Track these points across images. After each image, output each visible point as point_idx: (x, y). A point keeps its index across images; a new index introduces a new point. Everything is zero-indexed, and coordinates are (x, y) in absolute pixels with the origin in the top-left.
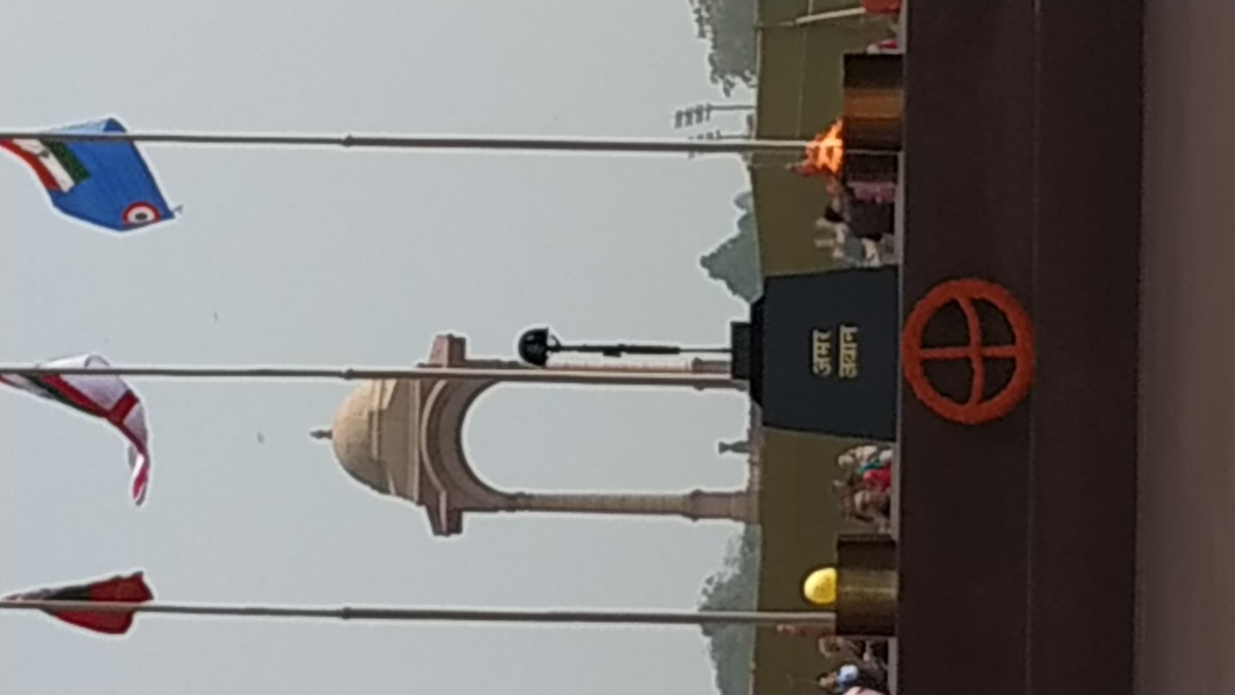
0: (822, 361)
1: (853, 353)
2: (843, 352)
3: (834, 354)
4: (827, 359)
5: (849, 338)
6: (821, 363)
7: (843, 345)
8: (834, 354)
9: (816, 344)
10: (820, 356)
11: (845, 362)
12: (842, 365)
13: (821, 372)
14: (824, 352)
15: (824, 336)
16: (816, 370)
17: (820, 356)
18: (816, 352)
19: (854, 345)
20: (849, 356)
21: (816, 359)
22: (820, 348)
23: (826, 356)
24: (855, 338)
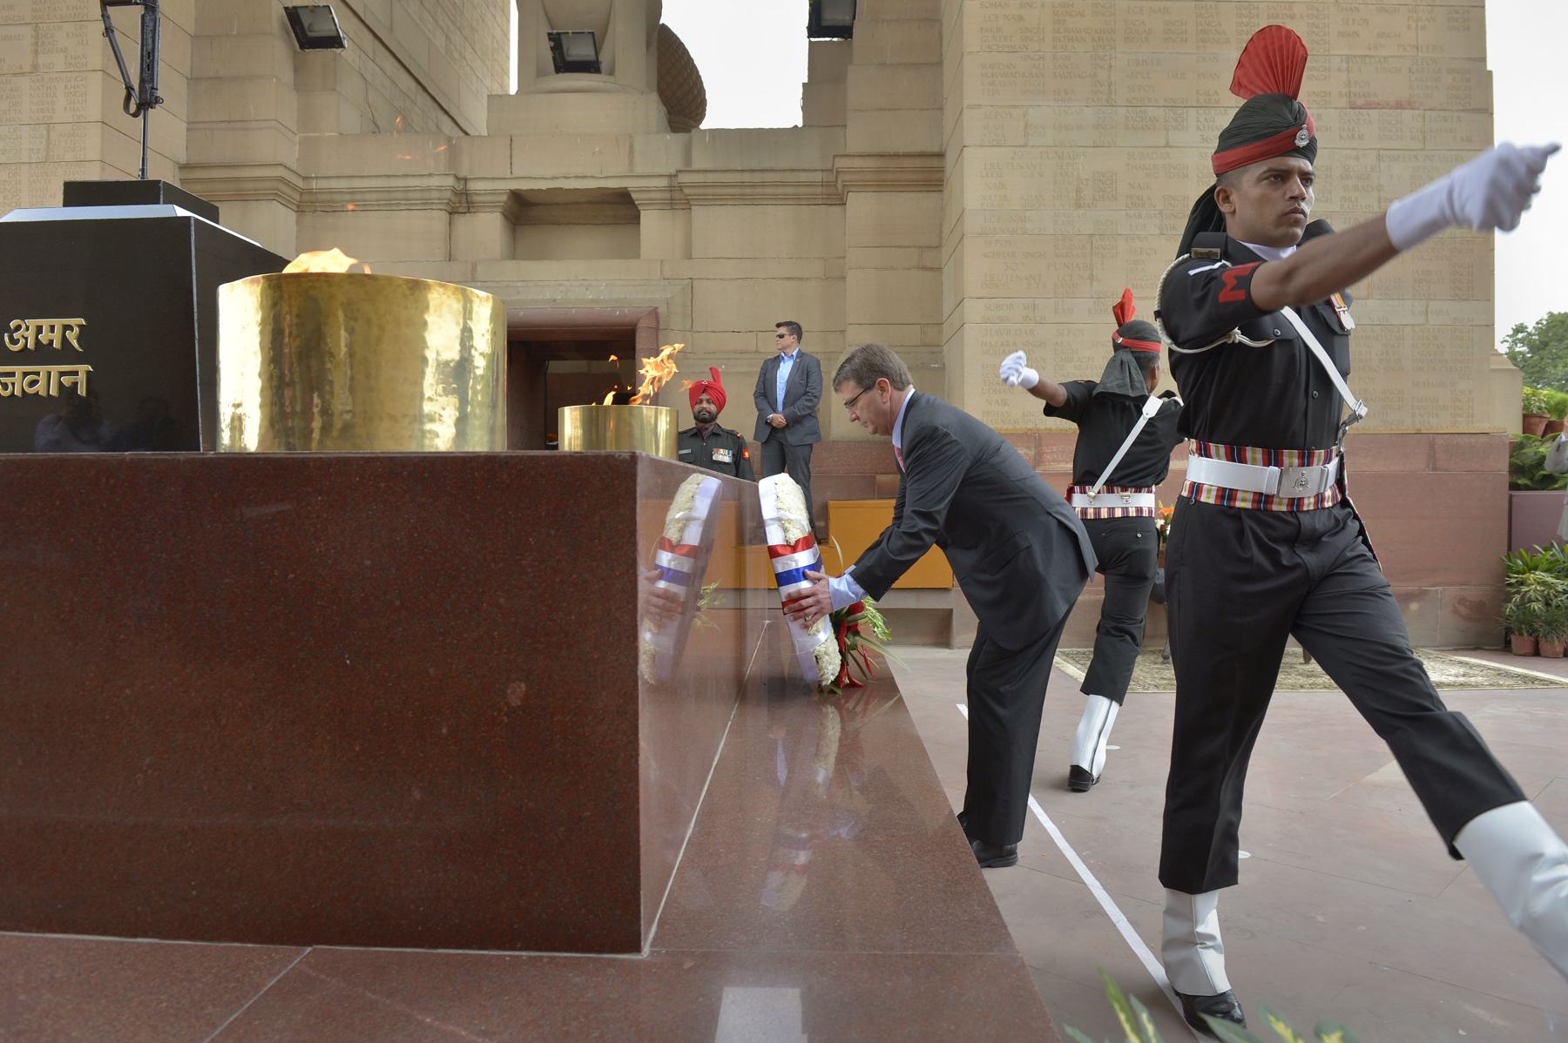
0: (31, 335)
1: (40, 388)
2: (43, 369)
3: (42, 354)
4: (31, 345)
5: (66, 381)
6: (27, 332)
7: (55, 369)
8: (42, 354)
9: (58, 323)
10: (39, 330)
11: (25, 374)
12: (18, 370)
13: (8, 330)
14: (44, 338)
15: (72, 337)
16: (13, 324)
17: (39, 330)
18: (45, 323)
19: (54, 391)
20: (33, 383)
21: (32, 323)
22: (53, 330)
23: (38, 342)
24: (68, 392)
